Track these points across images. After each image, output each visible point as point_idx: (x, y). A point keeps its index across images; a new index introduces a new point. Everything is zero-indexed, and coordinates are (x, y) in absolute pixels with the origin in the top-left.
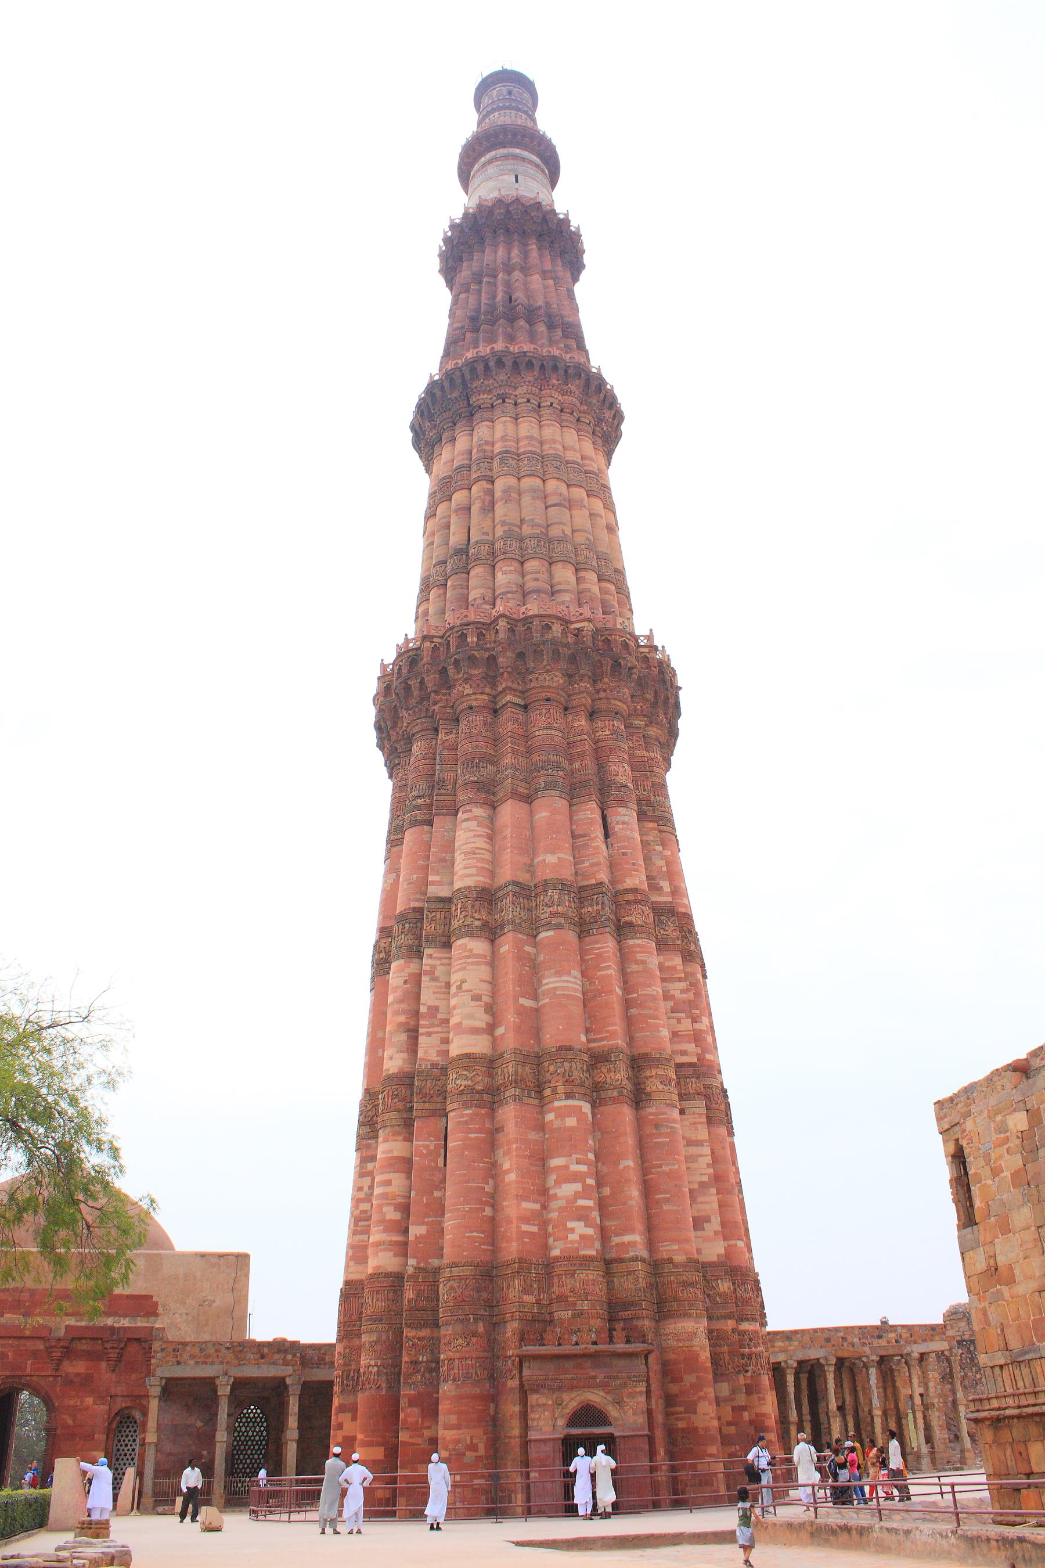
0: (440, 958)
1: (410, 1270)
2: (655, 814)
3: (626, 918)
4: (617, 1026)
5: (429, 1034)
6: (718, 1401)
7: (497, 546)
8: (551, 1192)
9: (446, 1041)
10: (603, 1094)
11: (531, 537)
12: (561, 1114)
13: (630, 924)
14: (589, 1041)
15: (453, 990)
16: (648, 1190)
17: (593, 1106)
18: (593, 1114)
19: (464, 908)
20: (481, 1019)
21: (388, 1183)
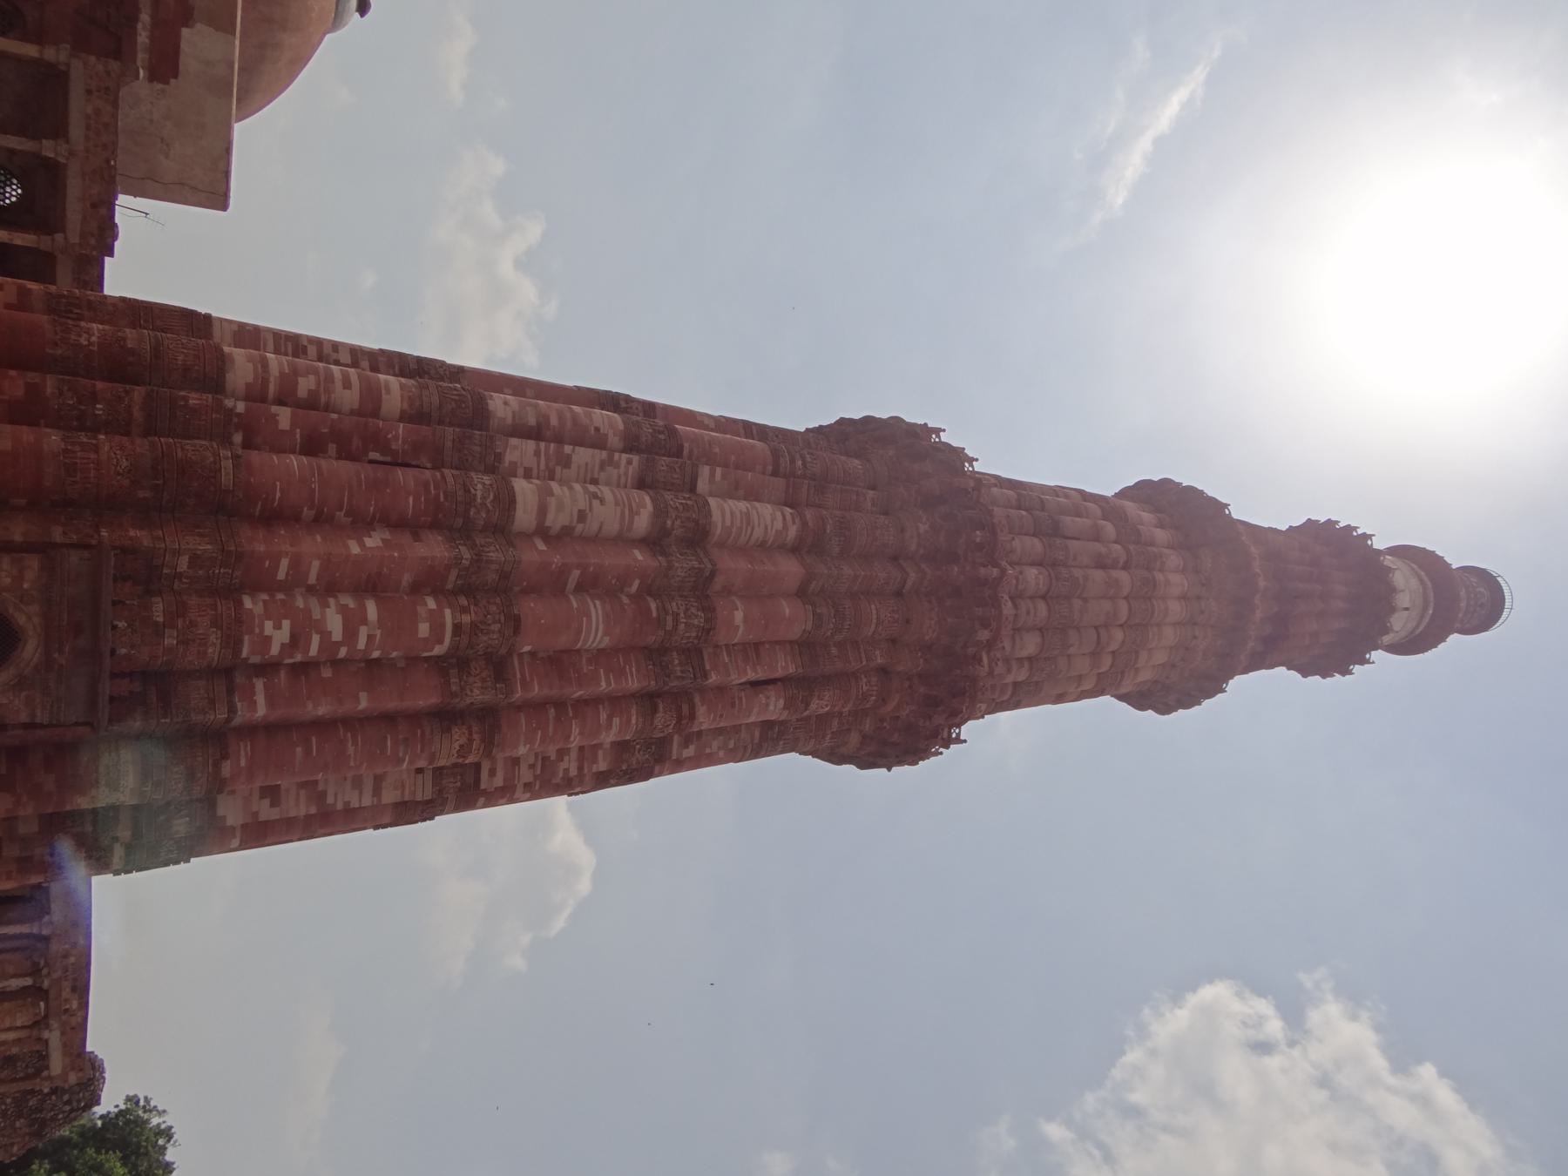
0: (626, 474)
1: (229, 403)
2: (768, 740)
3: (661, 706)
4: (536, 691)
5: (537, 453)
8: (332, 601)
9: (528, 475)
10: (454, 672)
13: (655, 710)
14: (521, 655)
15: (592, 488)
17: (438, 659)
18: (427, 659)
19: (686, 508)
20: (555, 520)
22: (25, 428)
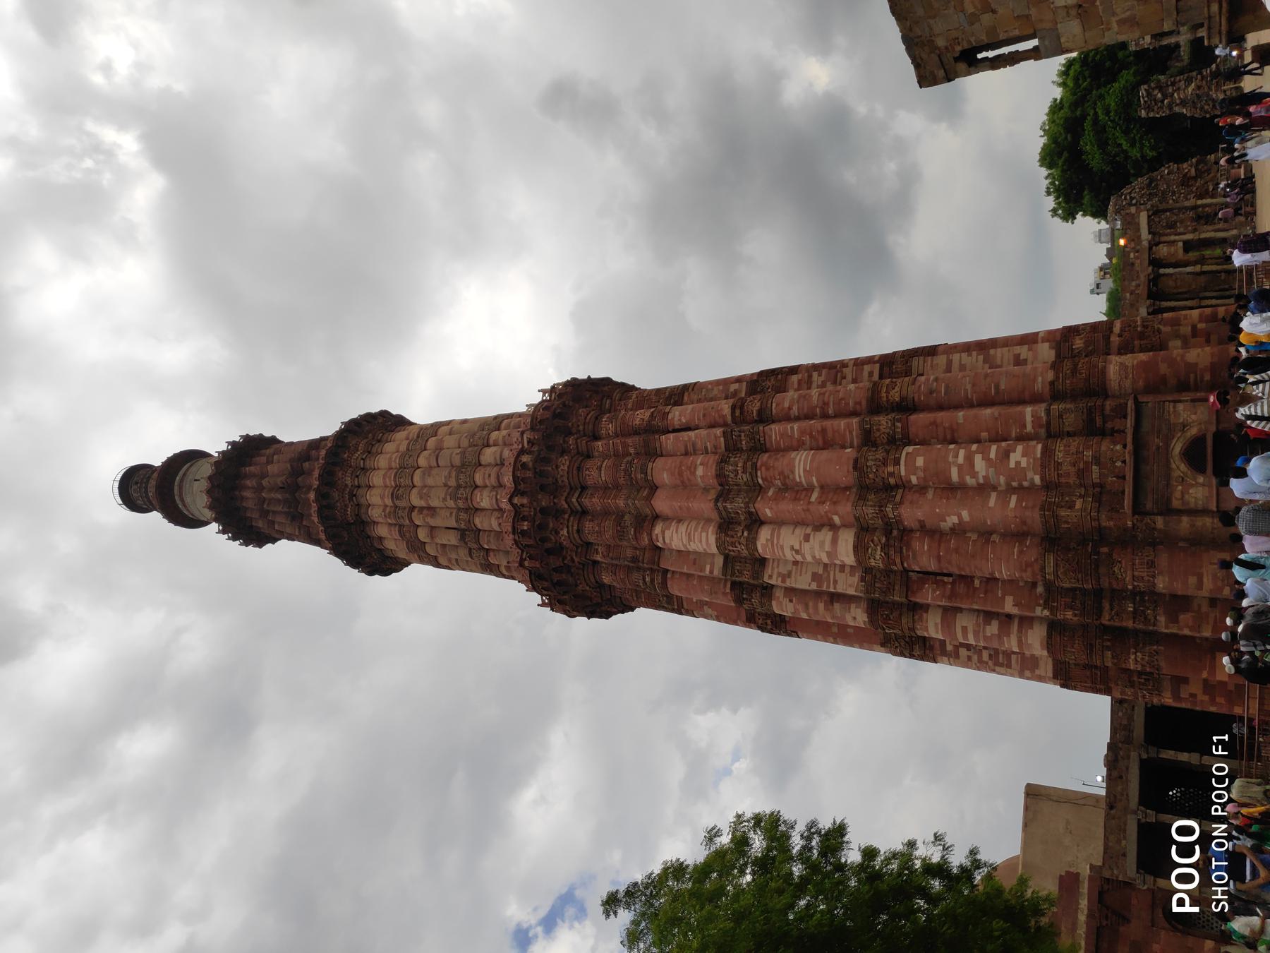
1: (1046, 613)
2: (677, 395)
4: (842, 424)
5: (835, 582)
6: (1186, 345)
7: (461, 504)
8: (981, 481)
9: (843, 567)
11: (457, 479)
12: (912, 469)
13: (760, 412)
15: (799, 558)
16: (986, 402)
17: (909, 444)
19: (733, 544)
20: (826, 535)
21: (964, 629)
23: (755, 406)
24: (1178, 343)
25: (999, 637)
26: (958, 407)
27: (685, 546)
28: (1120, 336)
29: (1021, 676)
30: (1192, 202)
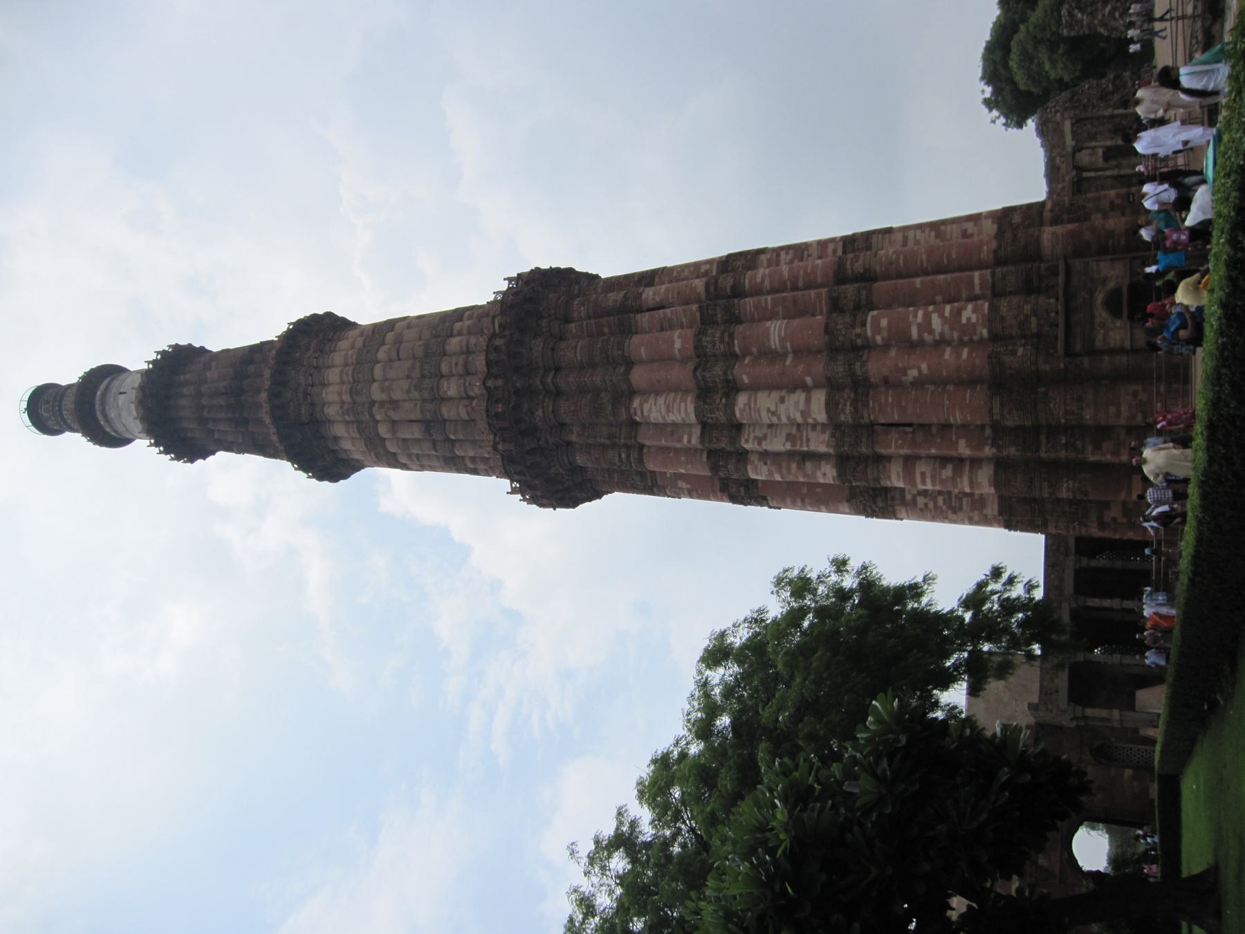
1: (994, 450)
5: (808, 440)
6: (1105, 216)
7: (426, 395)
9: (814, 427)
11: (422, 370)
12: (877, 328)
13: (733, 288)
14: (821, 314)
15: (775, 420)
16: (938, 271)
19: (712, 411)
20: (800, 396)
22: (1103, 423)
23: (725, 290)
24: (1099, 216)
25: (953, 479)
26: (916, 275)
27: (664, 418)
28: (1052, 211)
29: (972, 521)
30: (1108, 112)
